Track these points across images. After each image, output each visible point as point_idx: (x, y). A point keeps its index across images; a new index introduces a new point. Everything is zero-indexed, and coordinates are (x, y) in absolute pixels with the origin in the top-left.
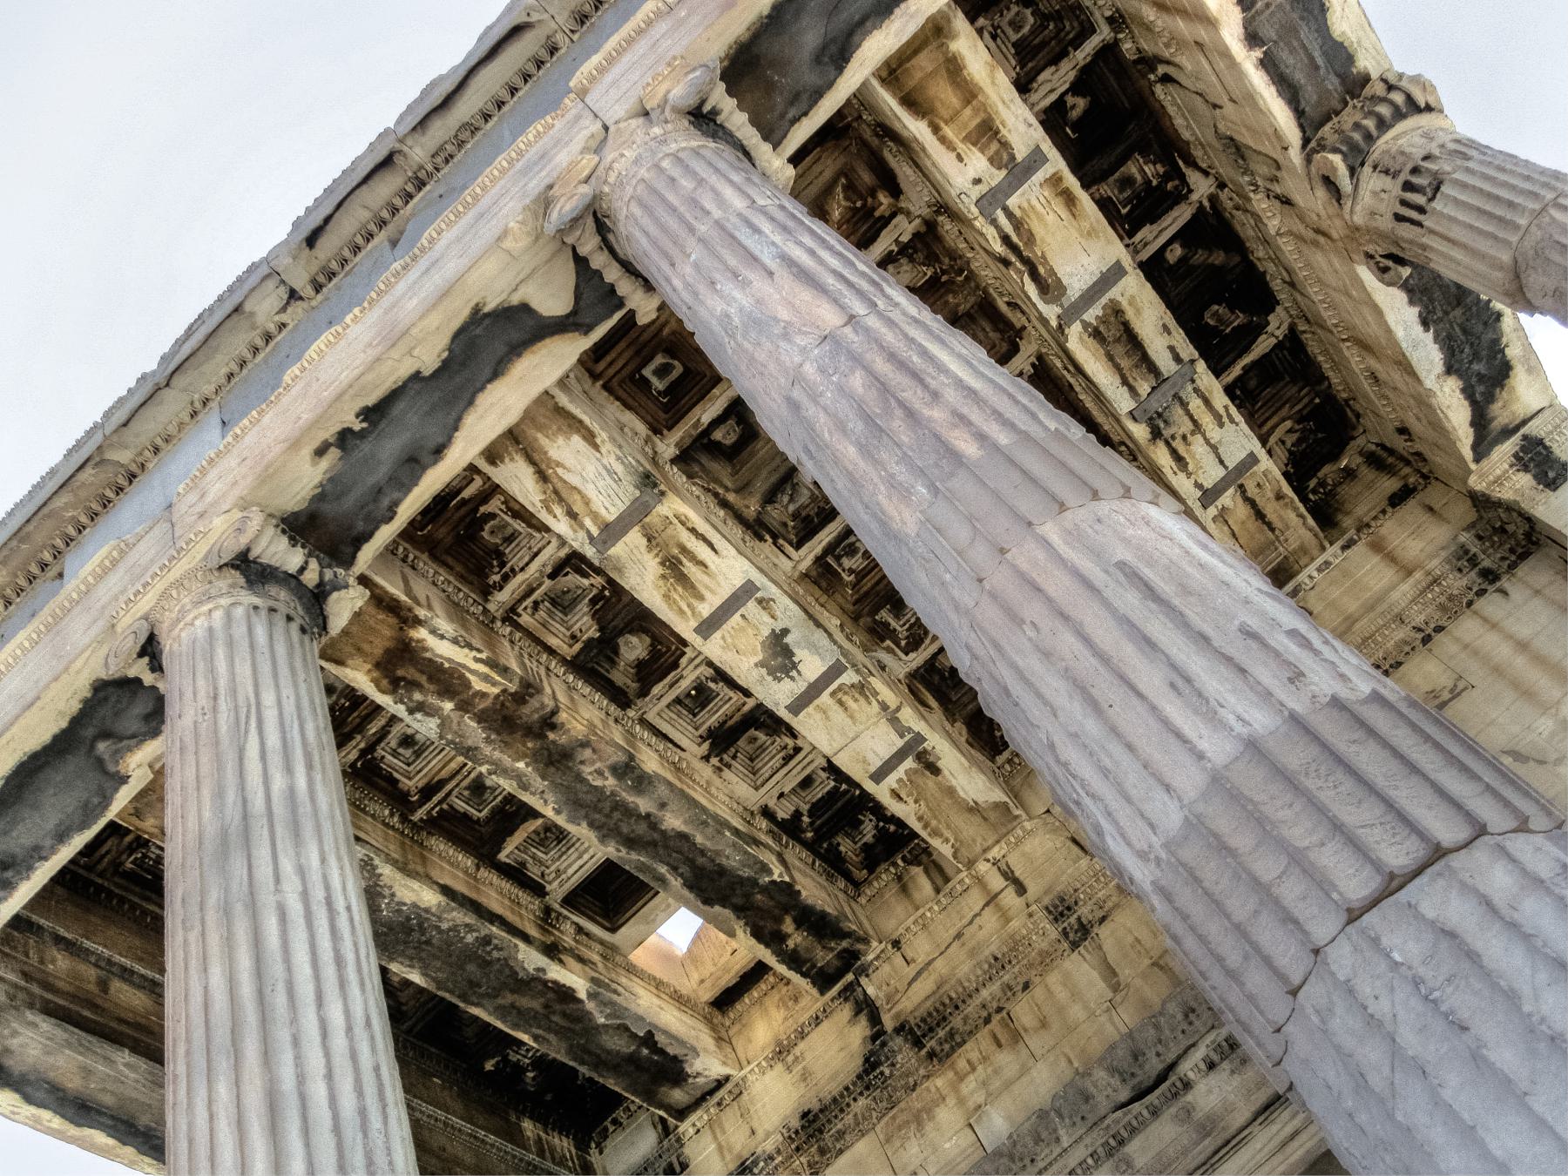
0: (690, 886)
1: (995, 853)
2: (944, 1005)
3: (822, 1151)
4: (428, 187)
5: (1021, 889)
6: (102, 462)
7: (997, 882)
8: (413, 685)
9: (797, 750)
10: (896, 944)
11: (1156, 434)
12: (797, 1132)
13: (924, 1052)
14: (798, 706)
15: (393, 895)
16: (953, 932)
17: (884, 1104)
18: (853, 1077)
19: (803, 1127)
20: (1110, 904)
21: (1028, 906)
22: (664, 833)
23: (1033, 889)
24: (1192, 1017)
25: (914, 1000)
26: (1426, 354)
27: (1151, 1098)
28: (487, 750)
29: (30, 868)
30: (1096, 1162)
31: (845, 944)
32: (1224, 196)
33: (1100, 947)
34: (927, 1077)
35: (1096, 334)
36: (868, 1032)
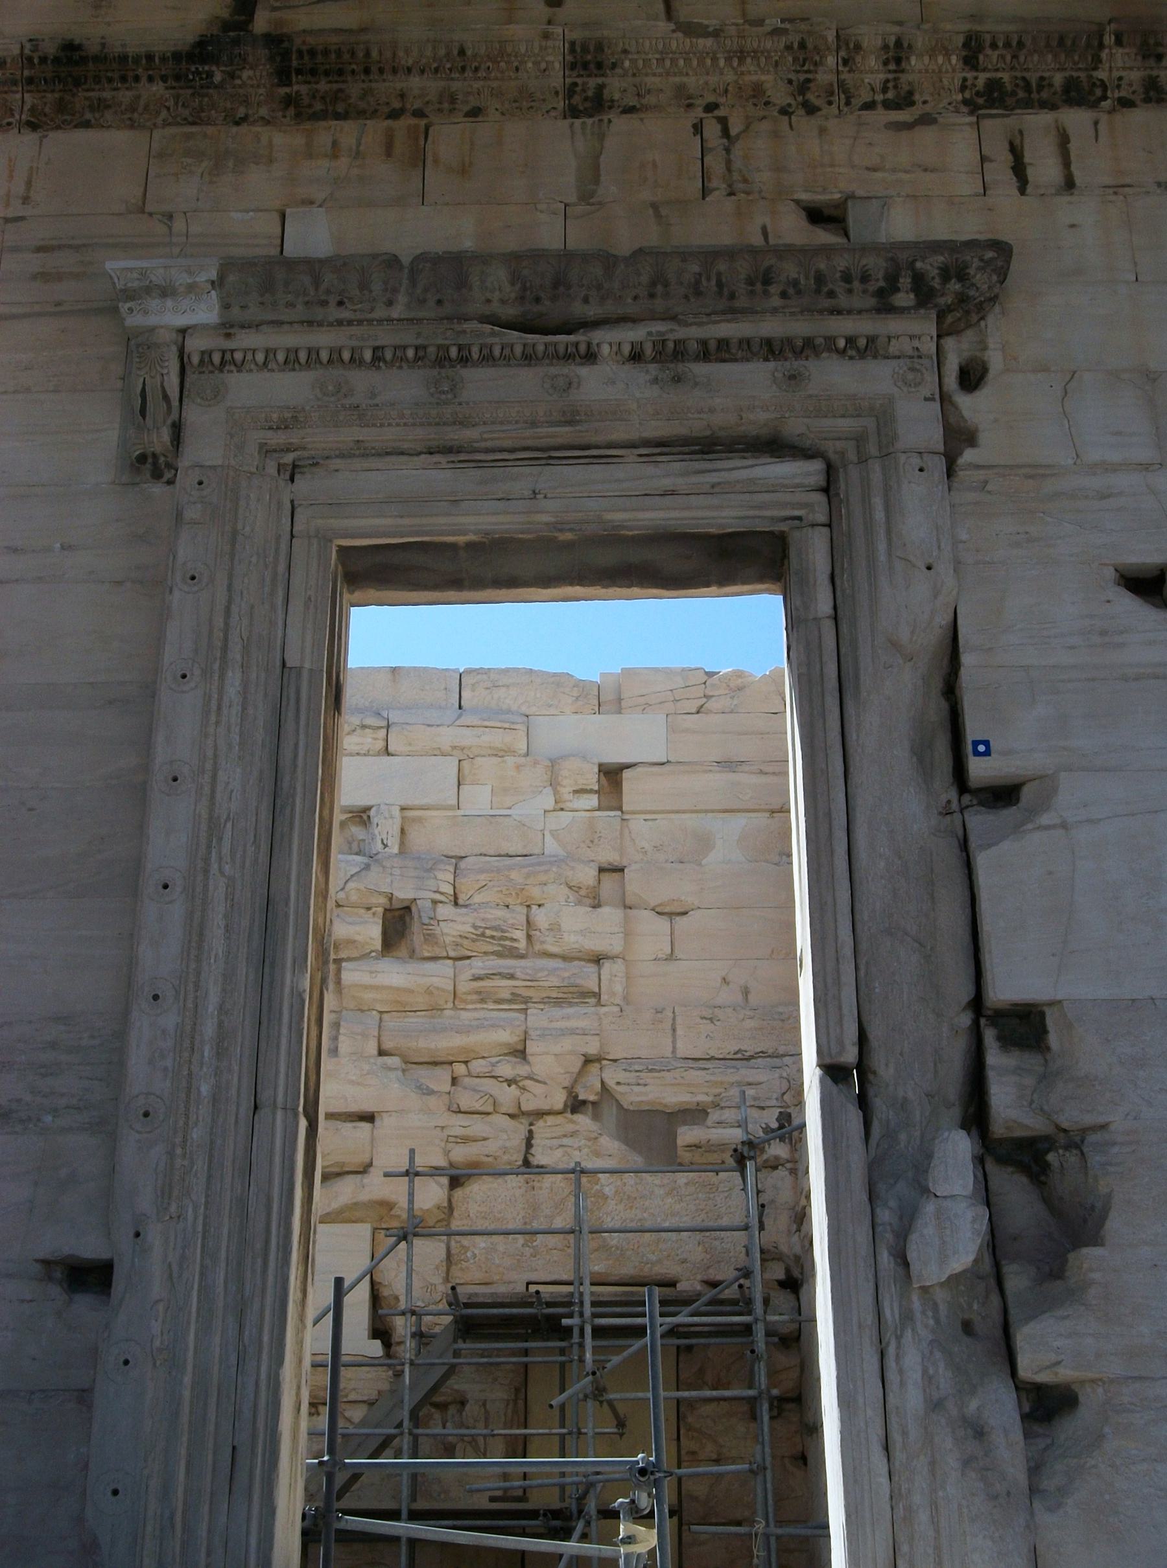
2: (353, 54)
3: (61, 107)
12: (43, 60)
13: (284, 91)
17: (186, 113)
19: (57, 60)
20: (651, 100)
21: (549, 23)
24: (660, 289)
27: (539, 340)
30: (417, 358)
33: (601, 137)
34: (268, 123)
36: (225, 14)
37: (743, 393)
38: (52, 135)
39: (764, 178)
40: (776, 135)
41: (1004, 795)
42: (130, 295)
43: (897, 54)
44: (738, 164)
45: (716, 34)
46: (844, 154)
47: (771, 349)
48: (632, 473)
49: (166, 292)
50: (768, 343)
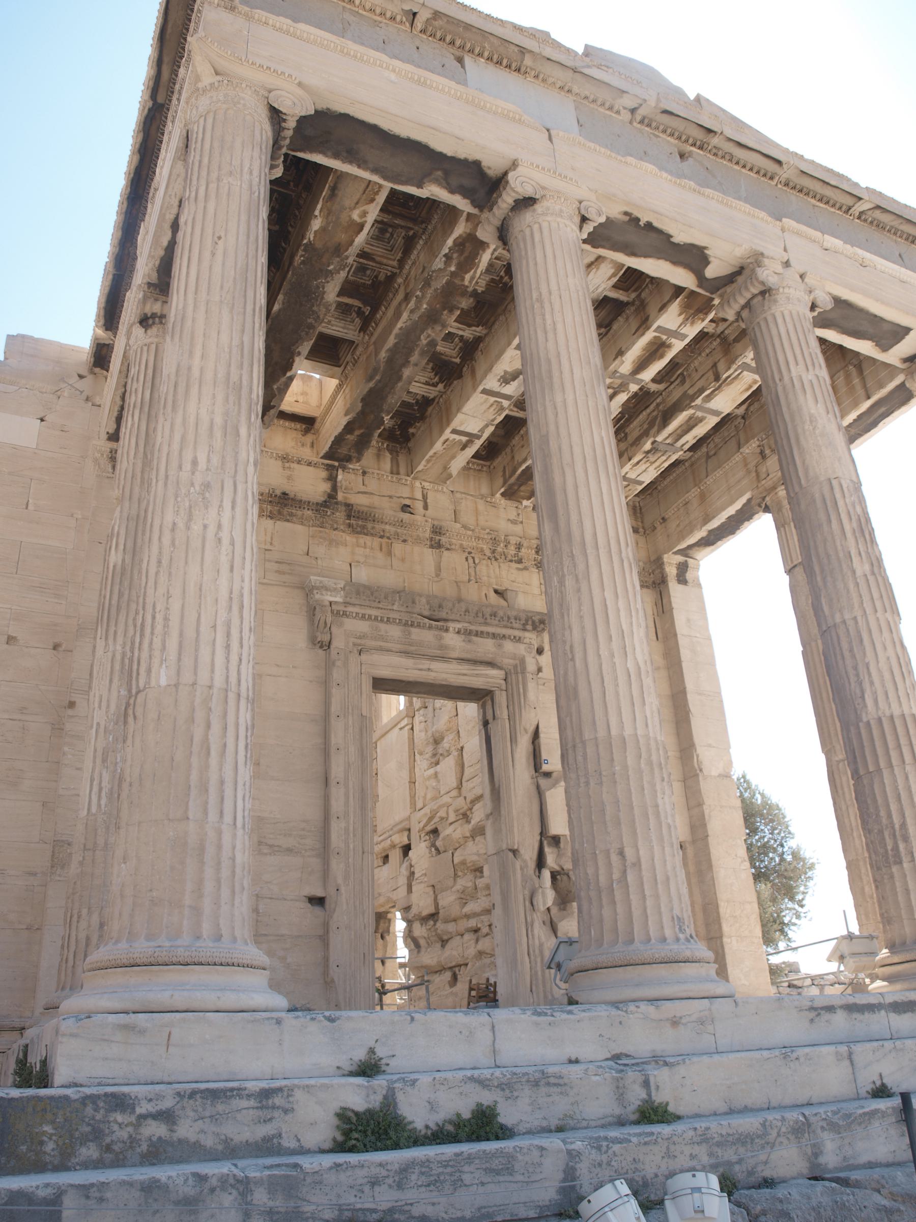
0: (371, 391)
1: (426, 485)
3: (280, 513)
4: (701, 152)
5: (426, 507)
6: (523, 53)
7: (419, 495)
8: (461, 252)
10: (364, 473)
11: (648, 452)
14: (485, 392)
15: (328, 282)
16: (389, 493)
18: (315, 501)
20: (453, 547)
22: (400, 370)
25: (359, 501)
26: (715, 523)
28: (430, 292)
29: (351, 162)
31: (355, 455)
32: (739, 420)
34: (344, 532)
35: (690, 418)
37: (485, 648)
38: (278, 522)
39: (485, 579)
40: (487, 566)
41: (548, 775)
42: (317, 588)
43: (519, 547)
44: (478, 573)
45: (473, 530)
46: (507, 575)
47: (494, 636)
48: (454, 667)
49: (327, 589)
50: (494, 634)
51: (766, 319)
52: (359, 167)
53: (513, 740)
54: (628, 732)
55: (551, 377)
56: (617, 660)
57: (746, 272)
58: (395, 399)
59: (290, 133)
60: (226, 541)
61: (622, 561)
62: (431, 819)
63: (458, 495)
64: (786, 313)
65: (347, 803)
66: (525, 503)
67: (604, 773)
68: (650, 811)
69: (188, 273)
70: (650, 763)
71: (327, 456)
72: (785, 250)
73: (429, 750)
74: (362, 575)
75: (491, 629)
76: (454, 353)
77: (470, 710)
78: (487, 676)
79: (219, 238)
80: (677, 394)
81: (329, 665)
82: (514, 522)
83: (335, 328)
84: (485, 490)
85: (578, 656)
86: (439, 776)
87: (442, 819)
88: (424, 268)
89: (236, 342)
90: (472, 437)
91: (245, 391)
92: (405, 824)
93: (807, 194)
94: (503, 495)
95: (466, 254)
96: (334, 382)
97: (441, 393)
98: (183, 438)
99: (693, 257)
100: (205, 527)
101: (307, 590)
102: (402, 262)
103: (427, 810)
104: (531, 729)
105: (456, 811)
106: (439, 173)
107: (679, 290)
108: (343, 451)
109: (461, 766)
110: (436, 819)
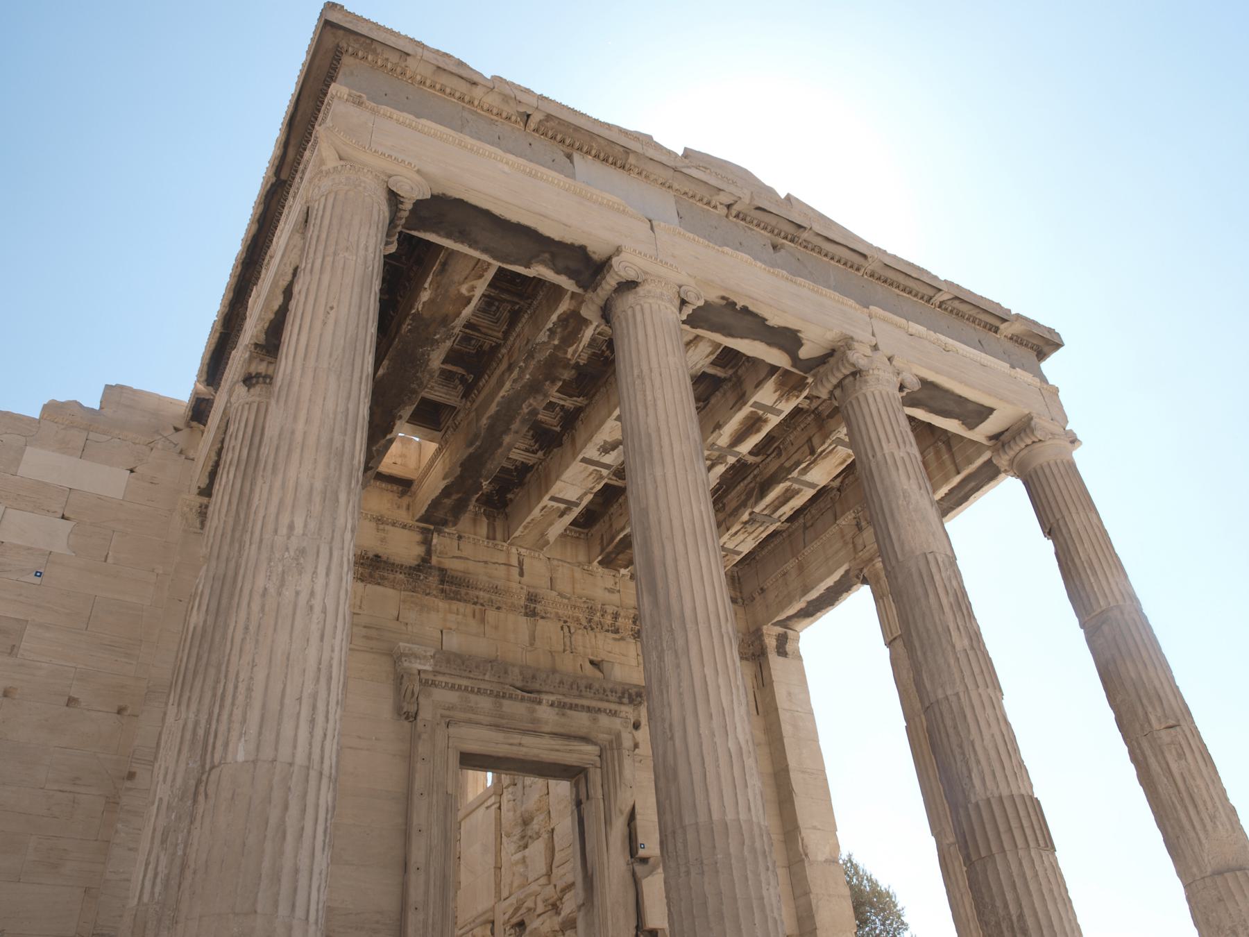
0: (470, 456)
1: (523, 551)
3: (371, 576)
5: (521, 574)
7: (515, 562)
9: (534, 452)
10: (460, 538)
11: (746, 523)
14: (584, 460)
16: (485, 559)
23: (525, 579)
25: (453, 565)
26: (814, 595)
28: (533, 363)
29: (462, 242)
32: (835, 492)
35: (787, 490)
37: (580, 721)
39: (580, 649)
41: (644, 860)
42: (406, 655)
43: (616, 616)
46: (603, 645)
47: (589, 709)
48: (547, 742)
49: (416, 656)
51: (857, 398)
52: (470, 246)
53: (608, 822)
54: (730, 816)
55: (651, 452)
56: (718, 740)
57: (837, 355)
58: (494, 465)
59: (406, 214)
60: (317, 609)
61: (722, 637)
62: (517, 910)
63: (555, 563)
64: (877, 393)
65: (427, 892)
66: (623, 571)
67: (705, 862)
68: (755, 904)
69: (298, 340)
70: (753, 850)
71: (421, 520)
72: (873, 335)
73: (518, 831)
74: (453, 642)
75: (585, 702)
76: (555, 422)
77: (561, 789)
78: (580, 752)
79: (332, 308)
80: (773, 467)
81: (414, 738)
82: (611, 591)
83: (438, 393)
84: (582, 557)
85: (678, 735)
86: (528, 860)
87: (529, 910)
88: (528, 341)
89: (341, 409)
90: (570, 505)
91: (347, 457)
92: (488, 916)
93: (891, 284)
94: (600, 563)
95: (569, 329)
96: (433, 446)
97: (541, 461)
98: (281, 502)
99: (788, 339)
100: (297, 593)
101: (395, 657)
102: (506, 334)
103: (513, 900)
104: (627, 810)
105: (545, 901)
106: (547, 255)
107: (773, 369)
108: (440, 514)
109: (551, 850)
110: (523, 910)
